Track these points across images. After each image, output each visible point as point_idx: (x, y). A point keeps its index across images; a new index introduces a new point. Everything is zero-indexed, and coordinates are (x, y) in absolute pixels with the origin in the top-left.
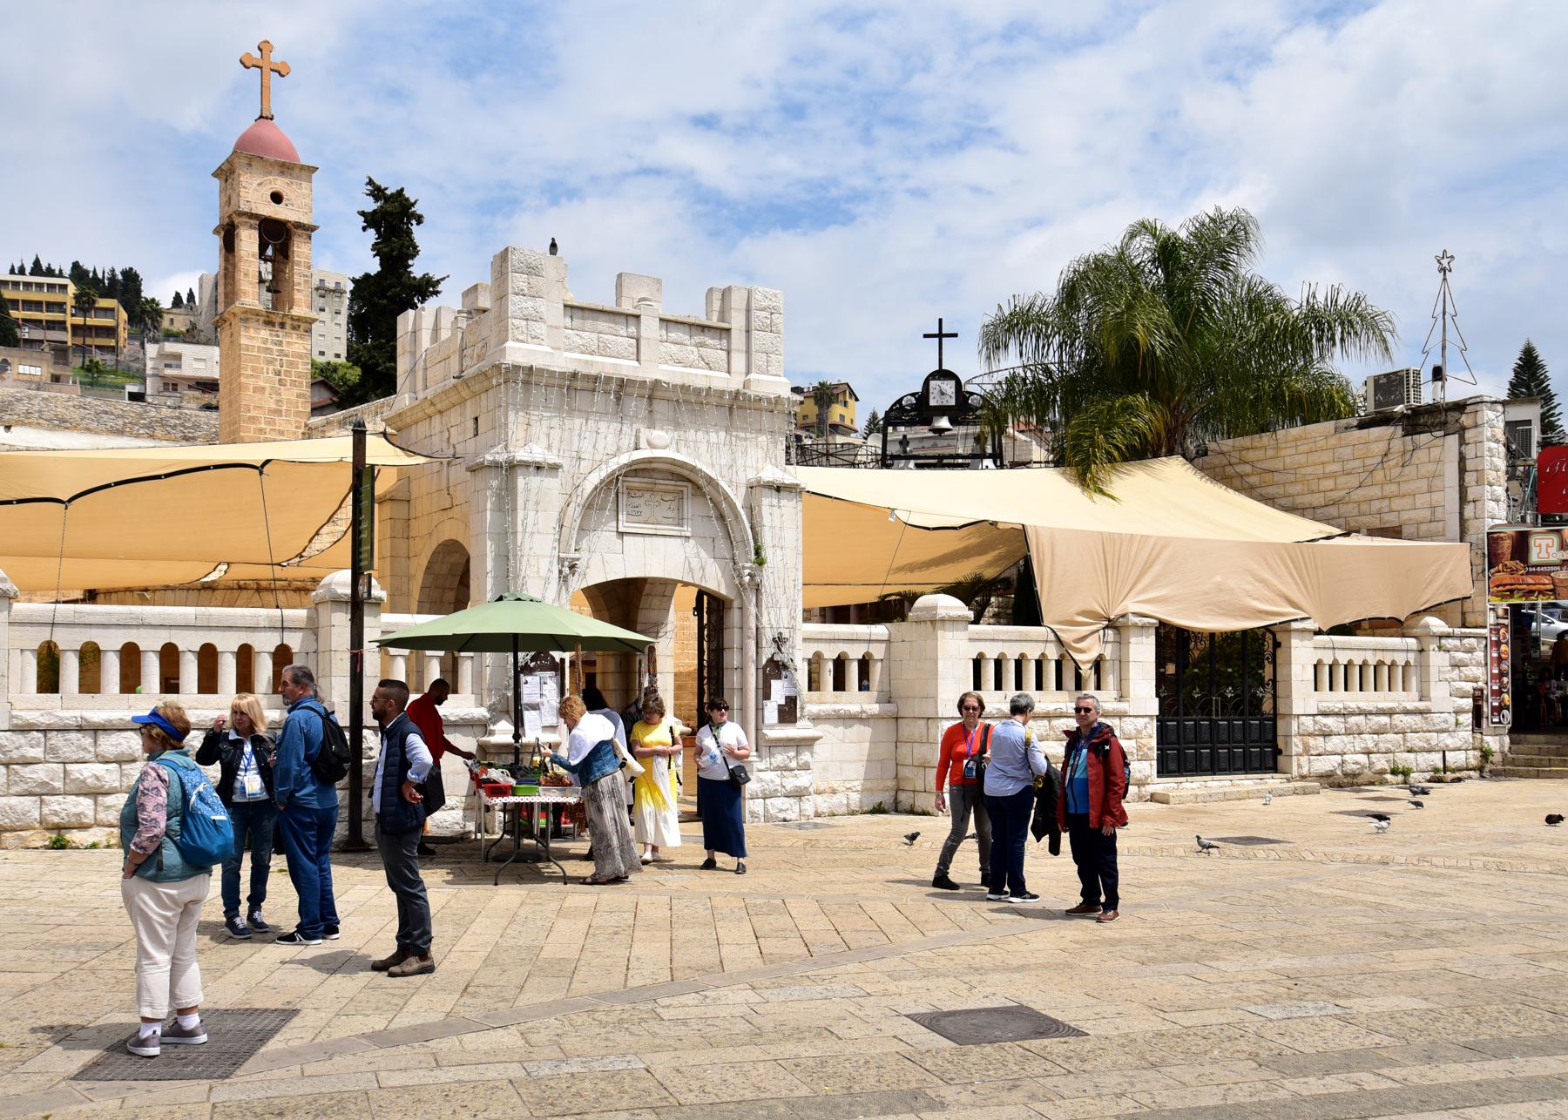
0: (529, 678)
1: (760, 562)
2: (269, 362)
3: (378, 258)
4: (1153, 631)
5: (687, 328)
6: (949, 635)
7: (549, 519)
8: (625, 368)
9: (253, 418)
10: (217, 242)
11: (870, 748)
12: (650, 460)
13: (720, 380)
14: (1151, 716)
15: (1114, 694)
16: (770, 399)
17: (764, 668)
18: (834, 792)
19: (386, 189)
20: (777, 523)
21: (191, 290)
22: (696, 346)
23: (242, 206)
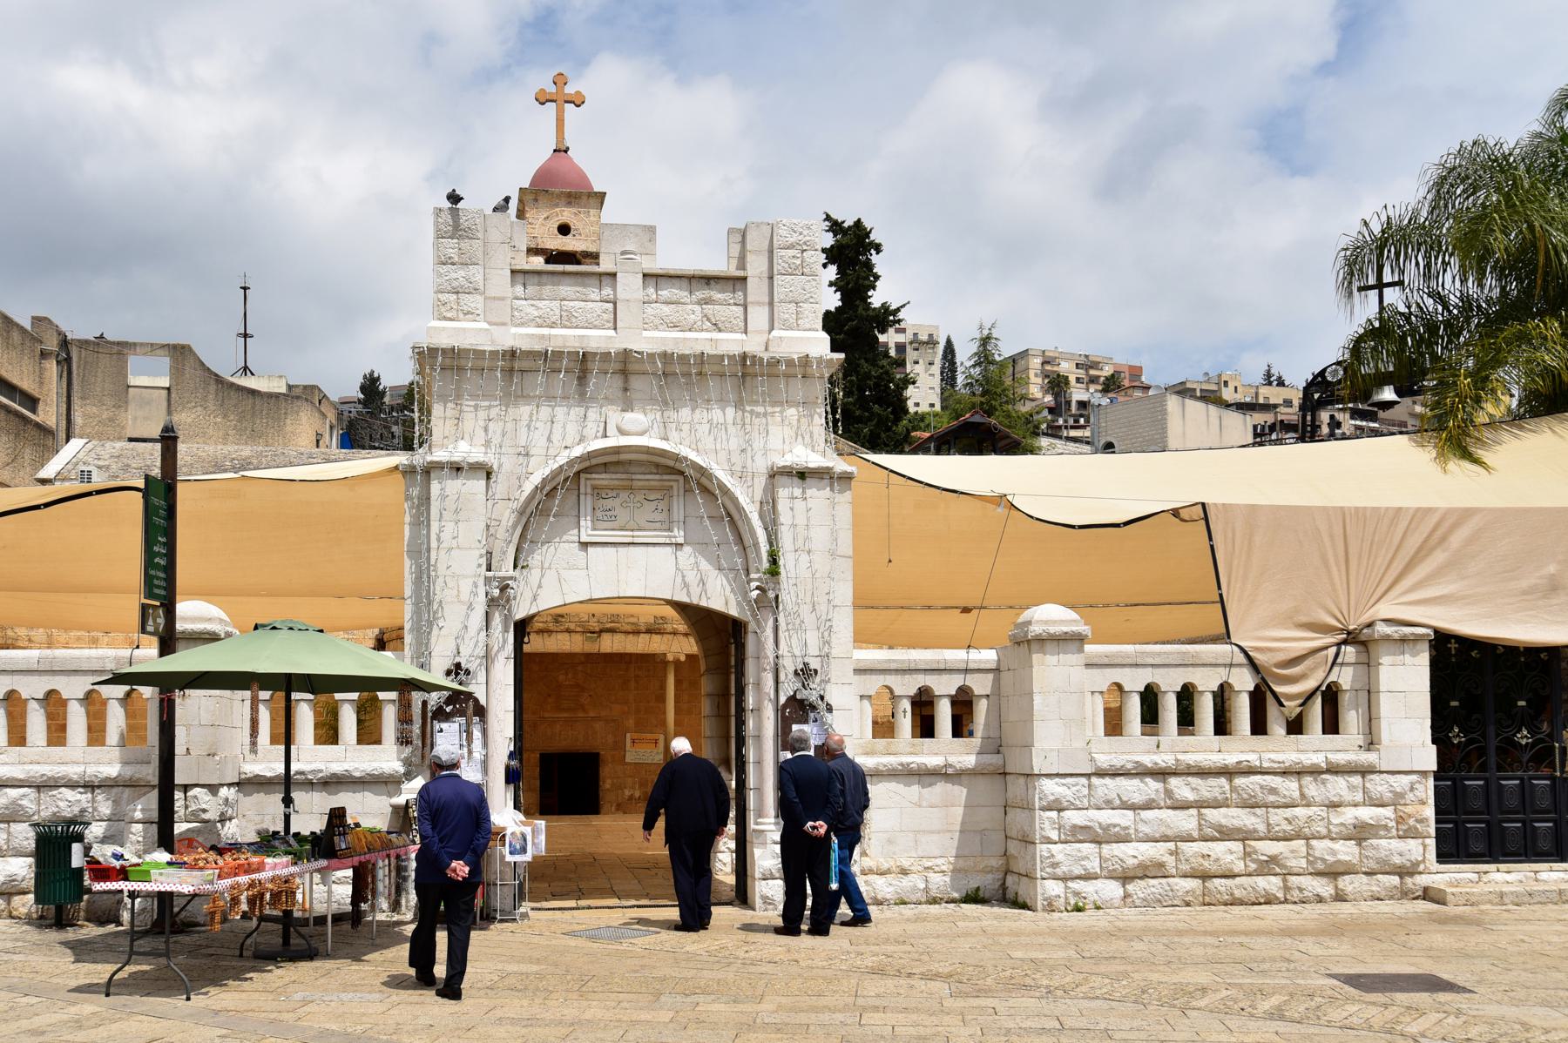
0: (444, 726)
1: (774, 571)
3: (839, 293)
4: (1426, 646)
5: (685, 283)
6: (1051, 659)
7: (472, 532)
8: (599, 339)
11: (965, 814)
12: (617, 450)
13: (731, 343)
14: (1424, 773)
15: (1360, 740)
16: (761, 359)
17: (785, 706)
18: (904, 872)
19: (844, 222)
20: (801, 520)
22: (699, 303)
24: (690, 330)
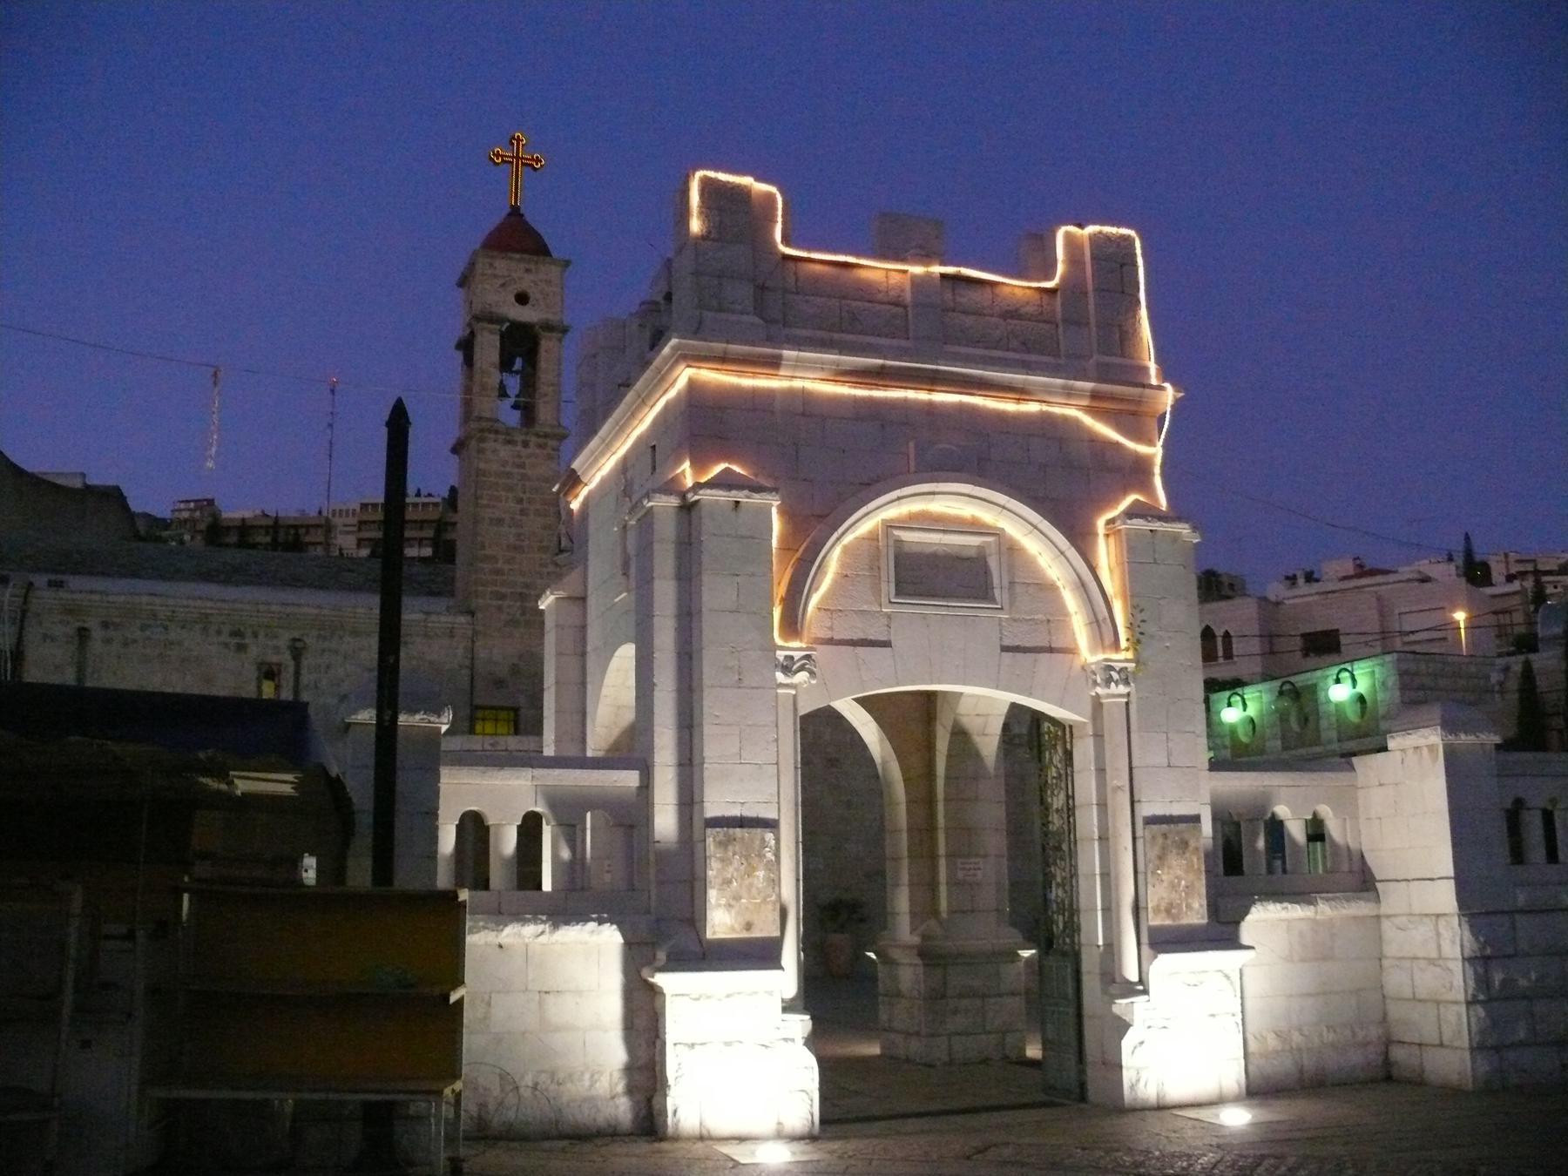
2: (510, 489)
10: (459, 356)
21: (400, 401)
24: (995, 348)
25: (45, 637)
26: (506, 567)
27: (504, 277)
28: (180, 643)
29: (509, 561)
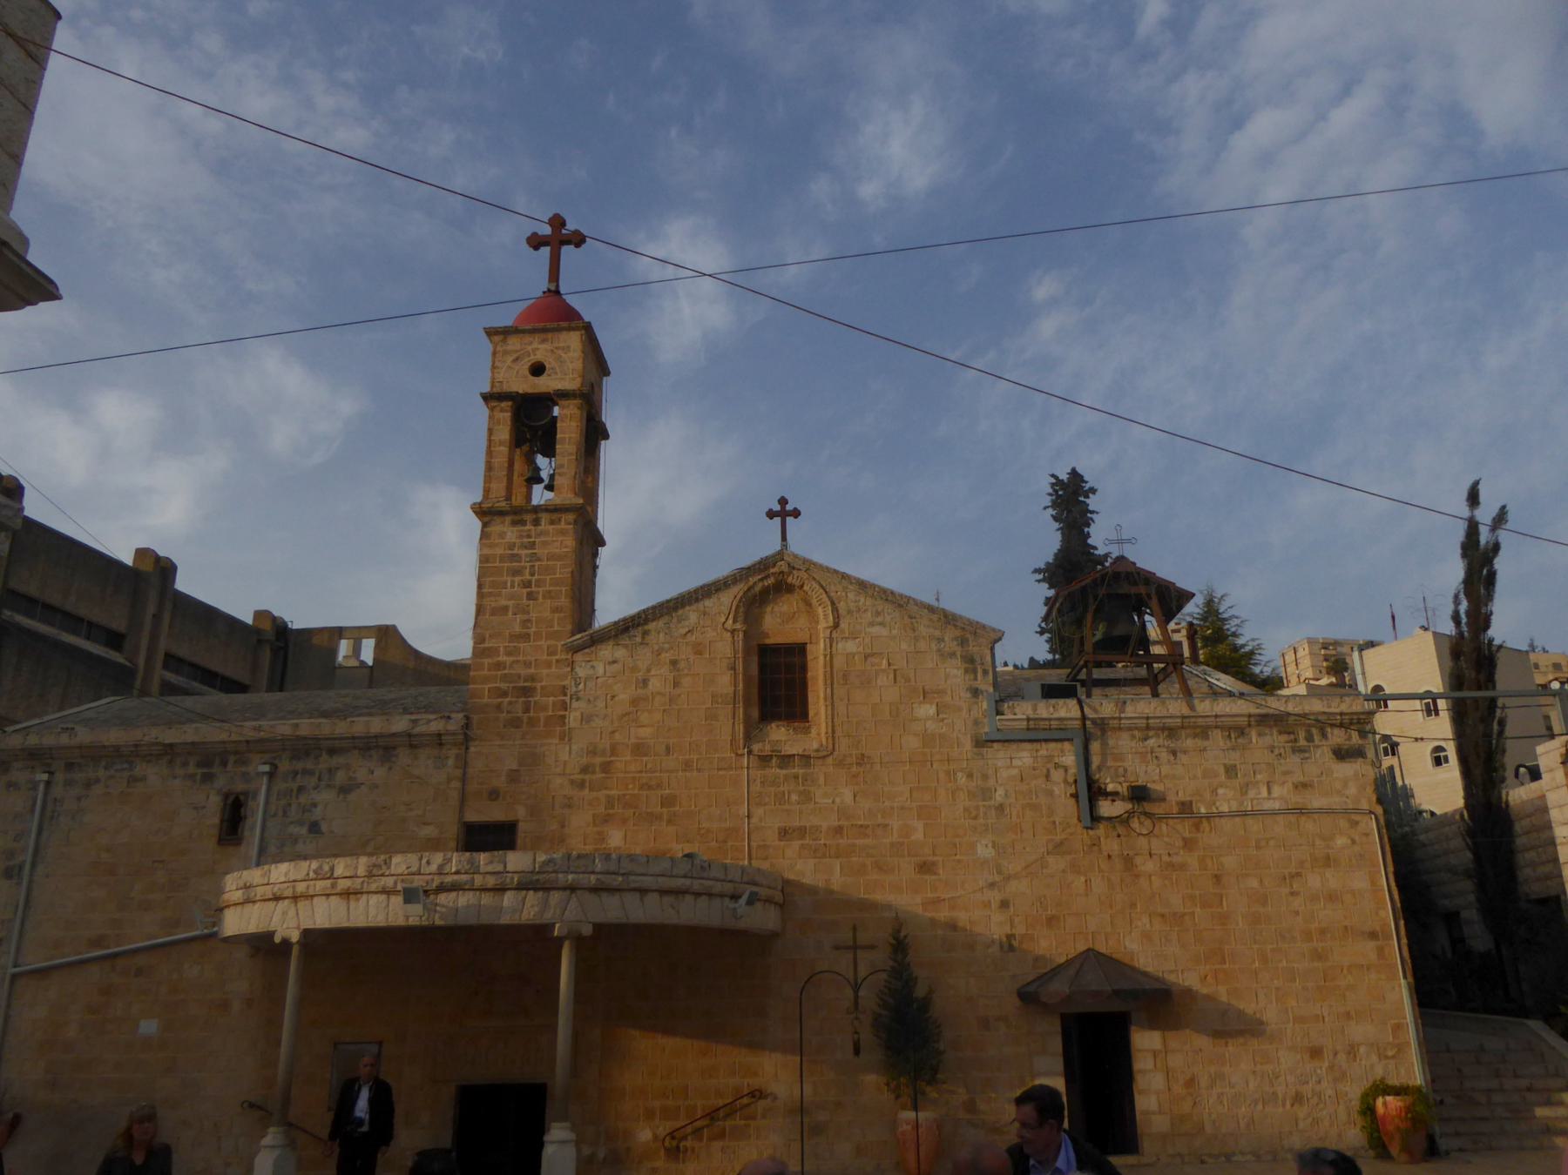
2: (516, 572)
9: (489, 649)
23: (505, 387)
25: (10, 785)
26: (508, 660)
27: (517, 351)
28: (144, 779)
29: (509, 654)
